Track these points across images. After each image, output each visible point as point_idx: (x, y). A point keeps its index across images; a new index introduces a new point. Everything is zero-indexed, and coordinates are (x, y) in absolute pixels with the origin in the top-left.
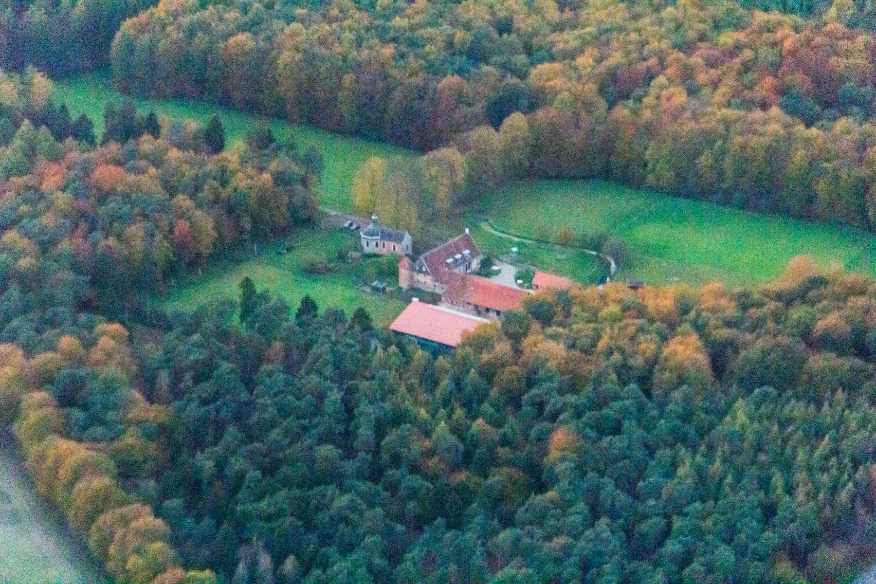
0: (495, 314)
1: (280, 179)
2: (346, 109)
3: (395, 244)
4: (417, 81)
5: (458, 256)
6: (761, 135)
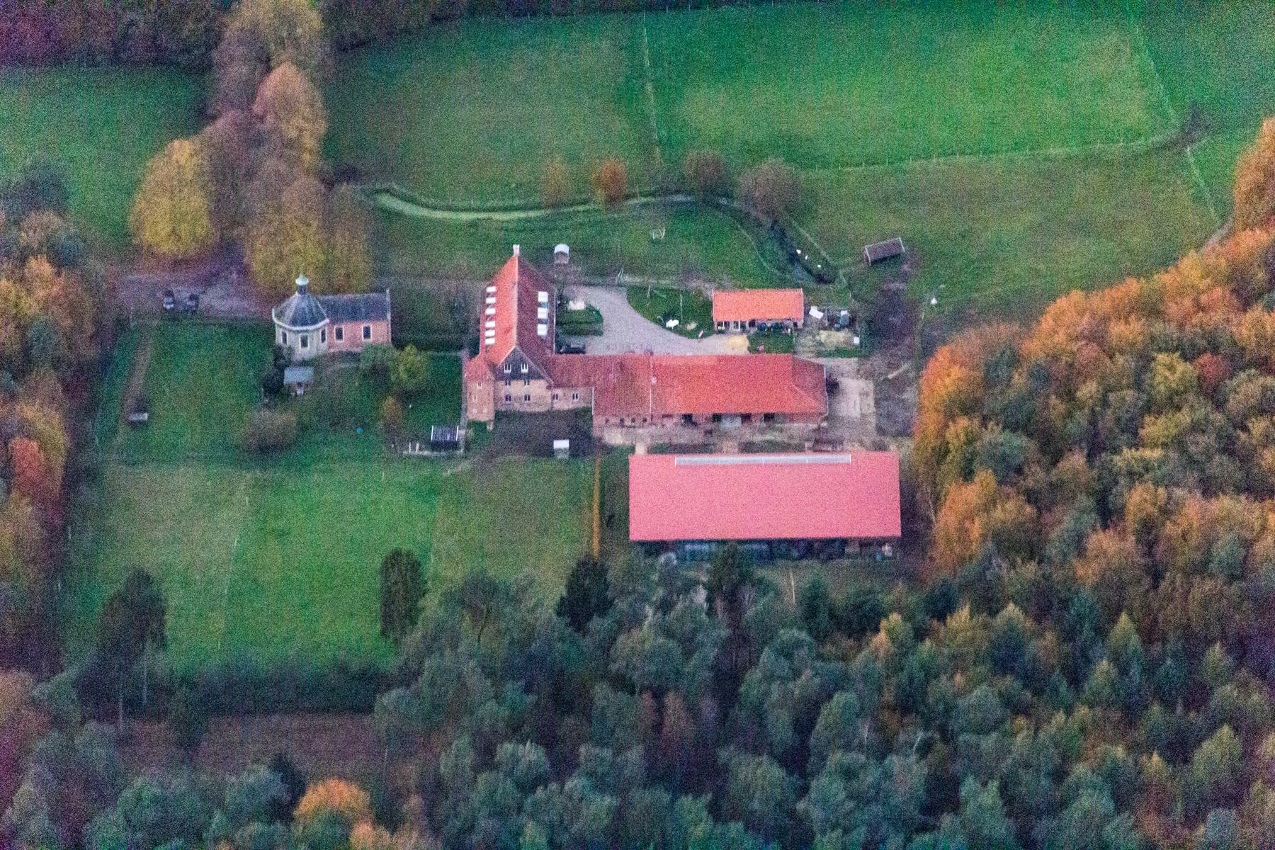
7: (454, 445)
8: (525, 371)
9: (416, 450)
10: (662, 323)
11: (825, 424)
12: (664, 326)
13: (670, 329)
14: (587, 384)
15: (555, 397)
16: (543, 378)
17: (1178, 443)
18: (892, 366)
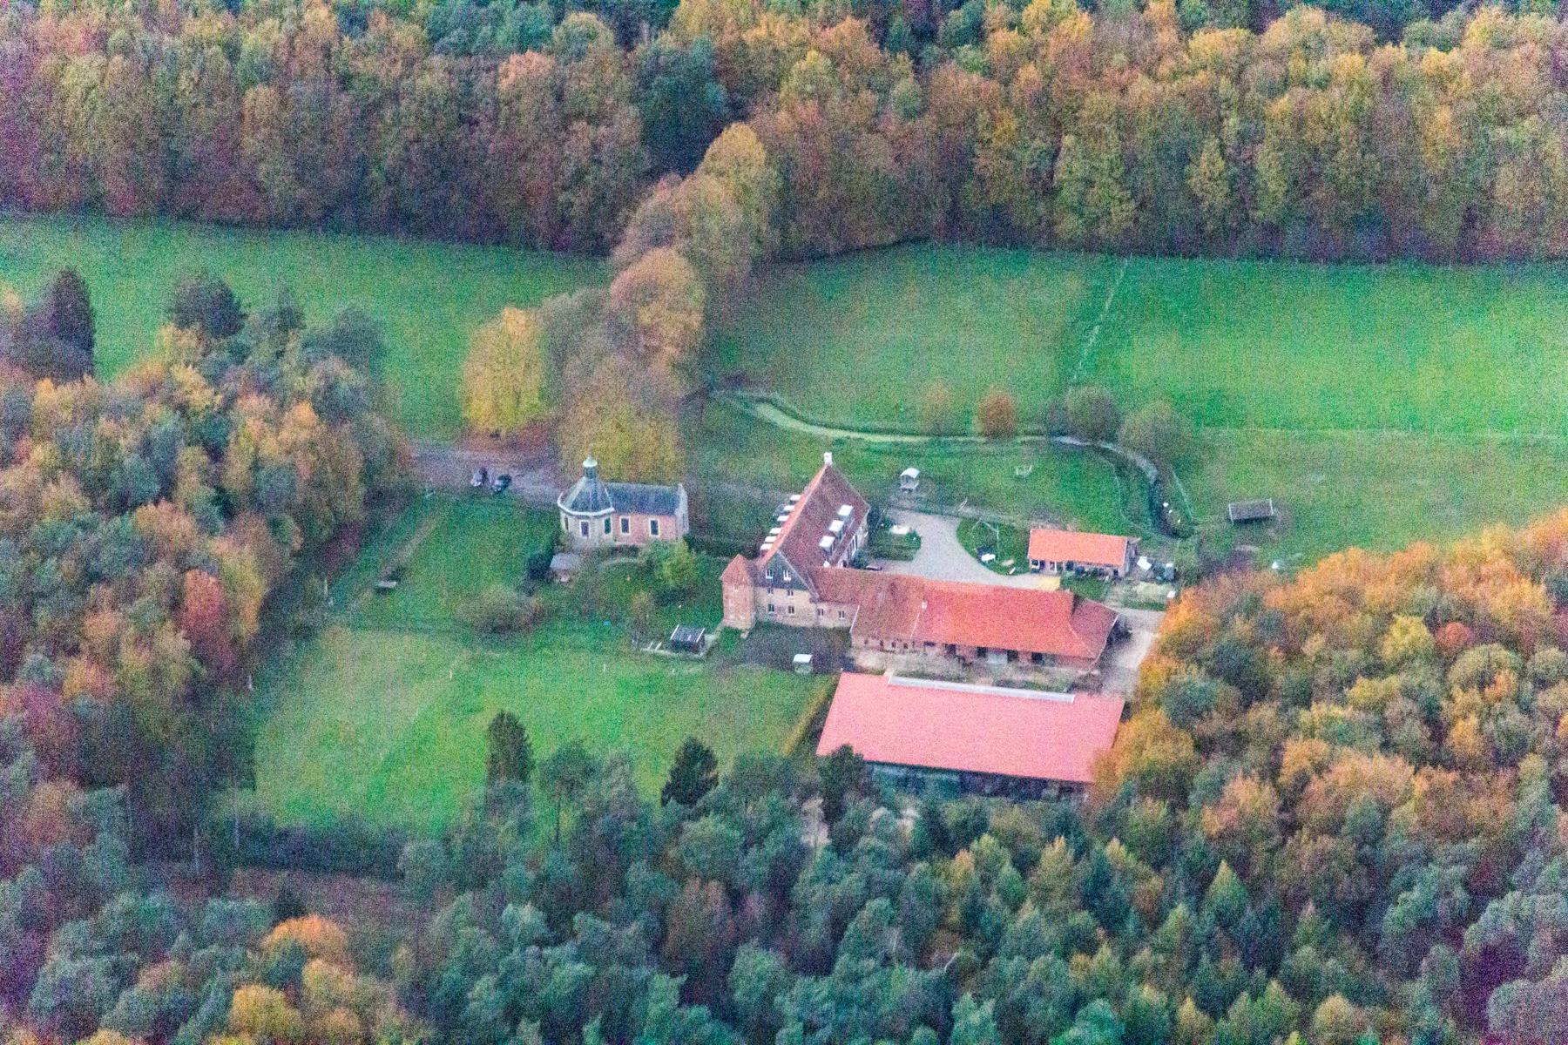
0: (1003, 659)
1: (332, 407)
2: (276, 174)
3: (659, 520)
4: (434, 77)
5: (836, 526)
6: (1324, 84)
8: (787, 578)
13: (984, 564)
15: (820, 612)
16: (805, 589)
17: (1378, 707)
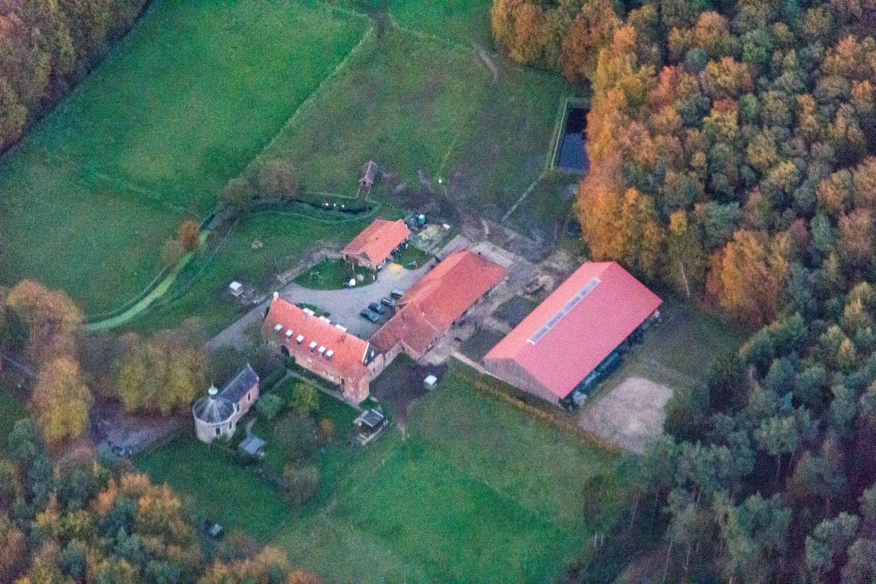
7: (380, 423)
9: (365, 439)
10: (347, 287)
11: (507, 278)
12: (349, 287)
14: (397, 341)
18: (480, 227)
